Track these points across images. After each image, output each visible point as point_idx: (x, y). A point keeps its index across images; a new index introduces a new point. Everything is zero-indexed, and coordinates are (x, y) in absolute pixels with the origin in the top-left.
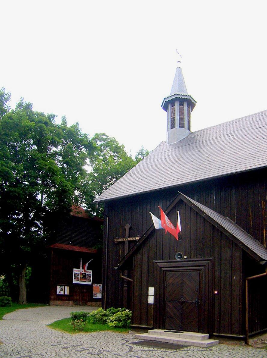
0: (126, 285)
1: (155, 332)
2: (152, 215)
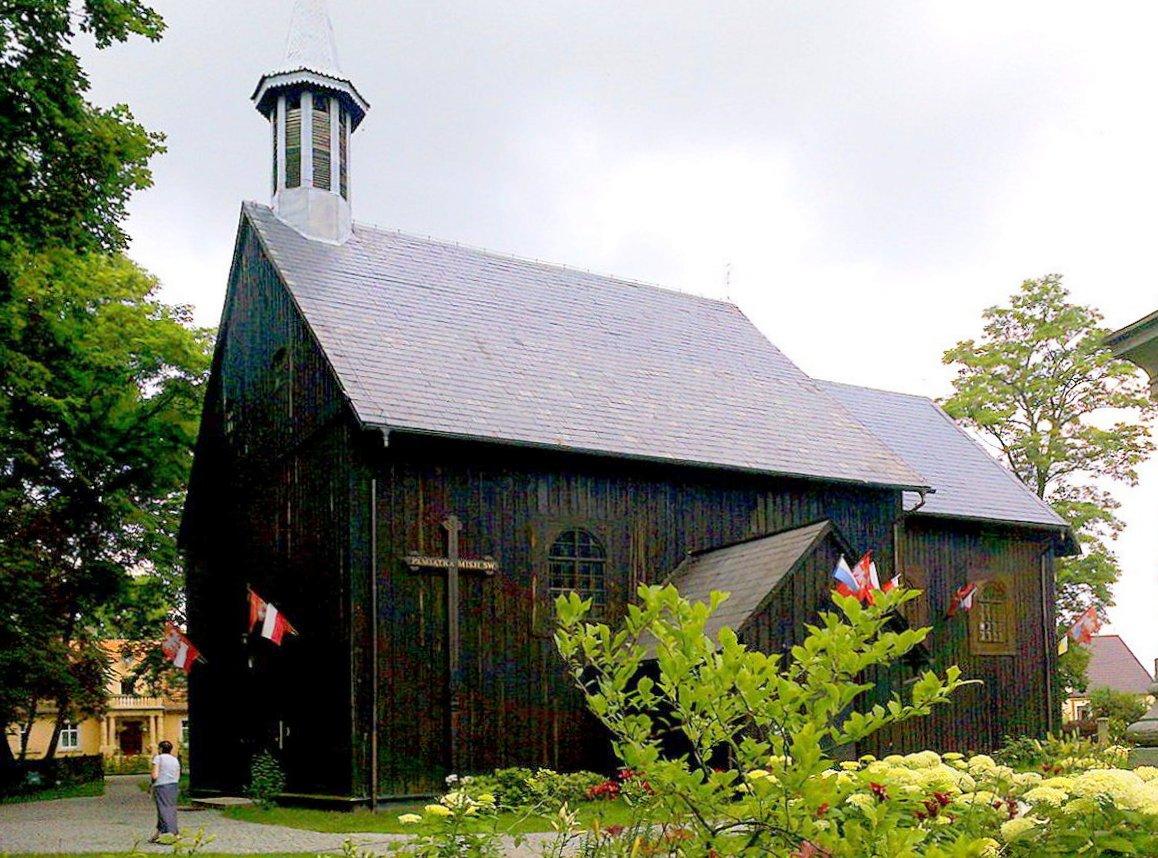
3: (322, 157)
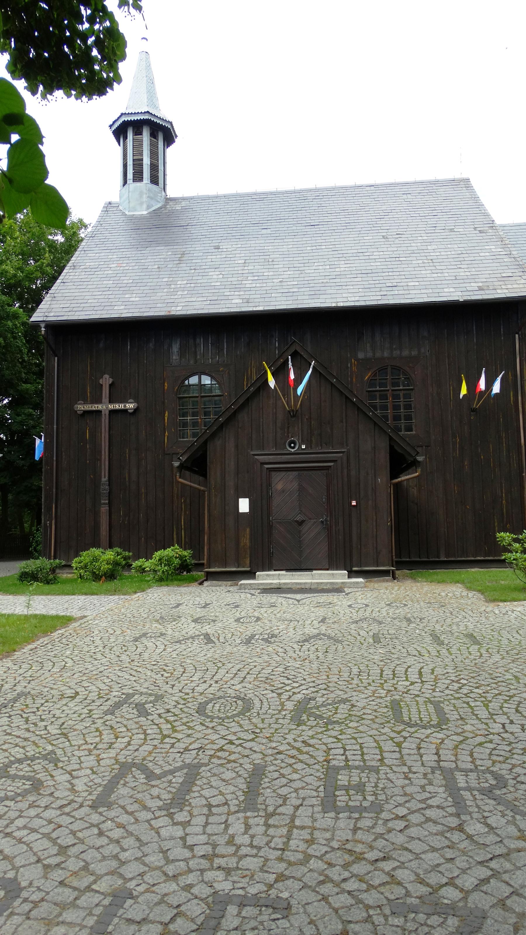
0: (105, 500)
1: (267, 575)
3: (138, 164)
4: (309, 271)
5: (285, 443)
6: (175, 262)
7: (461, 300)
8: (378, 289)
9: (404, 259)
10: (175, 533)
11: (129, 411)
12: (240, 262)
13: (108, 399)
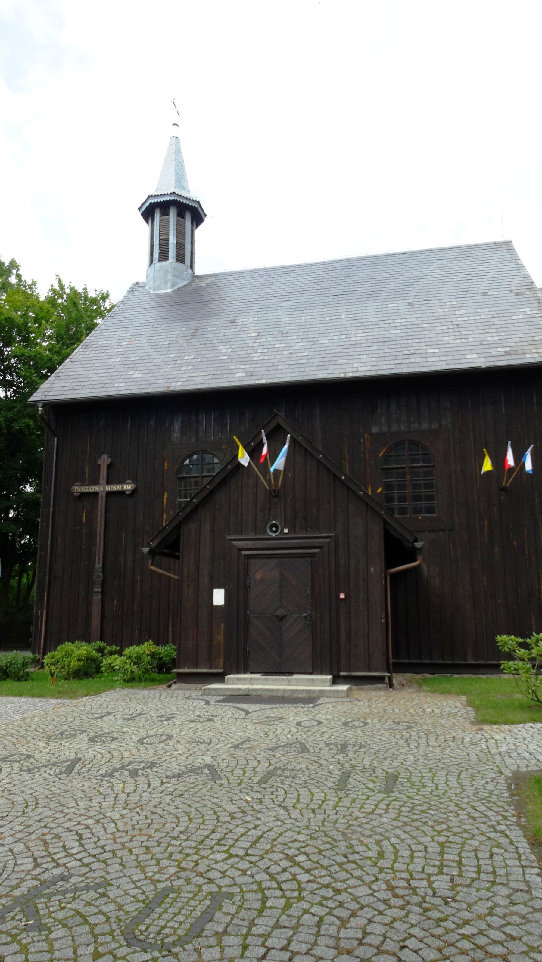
0: (99, 588)
1: (238, 679)
2: (241, 448)
4: (323, 342)
5: (265, 528)
6: (187, 338)
7: (484, 366)
8: (393, 358)
9: (428, 325)
10: (170, 625)
11: (127, 492)
12: (253, 335)
13: (105, 481)
